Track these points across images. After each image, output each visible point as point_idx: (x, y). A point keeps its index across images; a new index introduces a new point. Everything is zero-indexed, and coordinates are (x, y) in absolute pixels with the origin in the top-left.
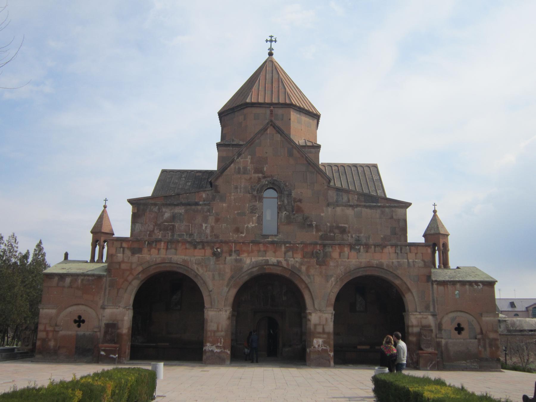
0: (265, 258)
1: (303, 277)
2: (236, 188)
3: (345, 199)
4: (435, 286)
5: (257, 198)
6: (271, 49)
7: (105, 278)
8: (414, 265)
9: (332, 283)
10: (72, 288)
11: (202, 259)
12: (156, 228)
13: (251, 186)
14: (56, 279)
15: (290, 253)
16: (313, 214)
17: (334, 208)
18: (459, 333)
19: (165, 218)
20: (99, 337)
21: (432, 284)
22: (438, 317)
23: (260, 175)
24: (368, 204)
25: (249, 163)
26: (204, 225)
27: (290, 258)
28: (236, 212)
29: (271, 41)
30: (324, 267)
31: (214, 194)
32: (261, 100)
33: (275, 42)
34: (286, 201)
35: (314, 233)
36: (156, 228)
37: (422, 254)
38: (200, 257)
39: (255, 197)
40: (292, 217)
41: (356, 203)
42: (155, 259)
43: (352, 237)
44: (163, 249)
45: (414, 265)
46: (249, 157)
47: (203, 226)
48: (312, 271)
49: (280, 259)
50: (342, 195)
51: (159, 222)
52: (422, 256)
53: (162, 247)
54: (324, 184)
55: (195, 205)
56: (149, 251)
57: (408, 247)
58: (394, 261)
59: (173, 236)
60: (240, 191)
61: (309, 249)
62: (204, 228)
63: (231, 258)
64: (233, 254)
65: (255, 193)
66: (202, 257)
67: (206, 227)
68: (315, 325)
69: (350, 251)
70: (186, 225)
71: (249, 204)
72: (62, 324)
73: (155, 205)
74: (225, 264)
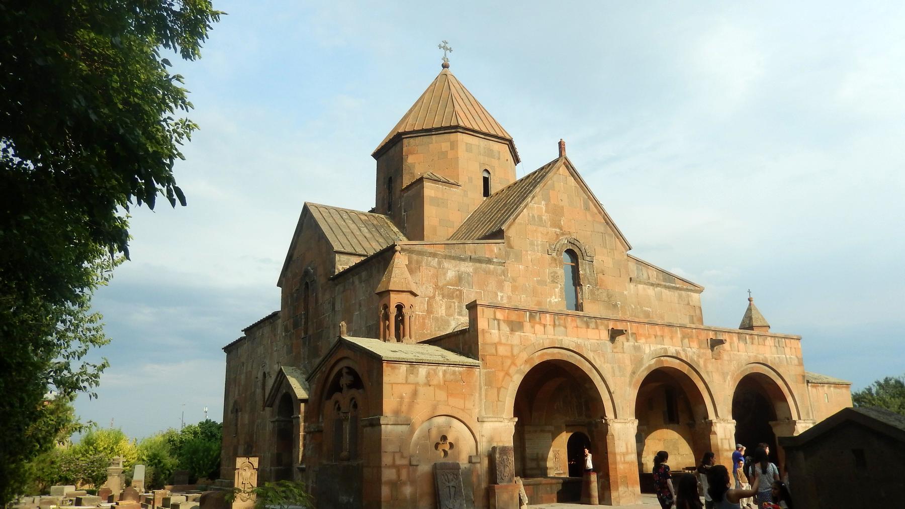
0: (663, 346)
2: (532, 244)
3: (645, 276)
5: (557, 262)
7: (478, 370)
8: (791, 362)
9: (729, 382)
10: (430, 386)
11: (598, 344)
12: (437, 293)
13: (549, 244)
14: (403, 368)
15: (686, 341)
16: (617, 291)
17: (636, 286)
19: (448, 279)
20: (479, 473)
23: (558, 230)
24: (668, 284)
25: (544, 211)
26: (500, 294)
27: (688, 348)
28: (535, 279)
30: (719, 361)
31: (508, 249)
34: (588, 272)
35: (620, 315)
36: (437, 293)
37: (795, 348)
38: (595, 341)
39: (555, 260)
42: (541, 341)
44: (550, 325)
48: (710, 367)
51: (440, 284)
52: (796, 351)
53: (548, 323)
55: (487, 264)
56: (533, 327)
57: (783, 340)
58: (775, 356)
59: (460, 307)
60: (538, 249)
61: (703, 336)
62: (499, 297)
63: (628, 343)
64: (630, 338)
65: (554, 254)
66: (597, 342)
67: (502, 297)
68: (722, 439)
69: (738, 341)
70: (477, 292)
71: (549, 270)
72: (417, 452)
73: (434, 255)
74: (624, 352)
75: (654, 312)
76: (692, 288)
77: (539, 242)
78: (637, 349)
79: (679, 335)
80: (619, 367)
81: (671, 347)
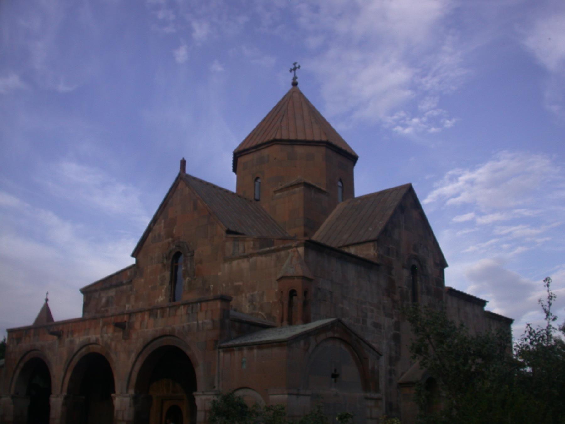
0: (88, 337)
1: (113, 356)
3: (241, 249)
4: (222, 354)
6: (295, 78)
15: (105, 329)
21: (219, 352)
23: (170, 239)
26: (127, 306)
28: (150, 286)
29: (295, 69)
32: (247, 147)
34: (189, 265)
41: (251, 251)
43: (246, 297)
46: (163, 221)
47: (125, 306)
65: (165, 261)
73: (96, 291)
79: (101, 324)
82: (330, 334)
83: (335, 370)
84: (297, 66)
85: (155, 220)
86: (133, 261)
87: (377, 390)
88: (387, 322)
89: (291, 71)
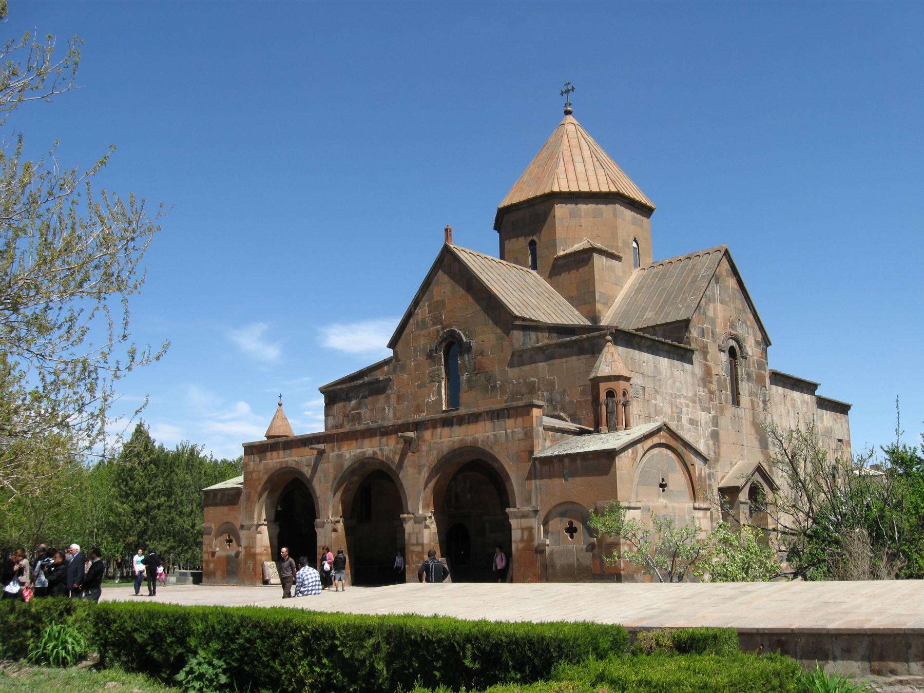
0: (361, 450)
5: (436, 360)
8: (513, 437)
15: (384, 439)
18: (572, 537)
22: (540, 513)
27: (385, 446)
29: (568, 91)
30: (417, 454)
33: (573, 91)
40: (474, 378)
45: (513, 437)
49: (375, 449)
50: (529, 334)
51: (347, 412)
54: (508, 321)
58: (489, 434)
68: (409, 534)
74: (329, 462)
75: (541, 382)
76: (595, 334)
77: (421, 346)
78: (340, 456)
80: (325, 475)
81: (369, 449)
82: (656, 440)
83: (663, 480)
84: (570, 88)
85: (416, 303)
86: (390, 353)
87: (705, 499)
88: (704, 417)
89: (562, 94)
